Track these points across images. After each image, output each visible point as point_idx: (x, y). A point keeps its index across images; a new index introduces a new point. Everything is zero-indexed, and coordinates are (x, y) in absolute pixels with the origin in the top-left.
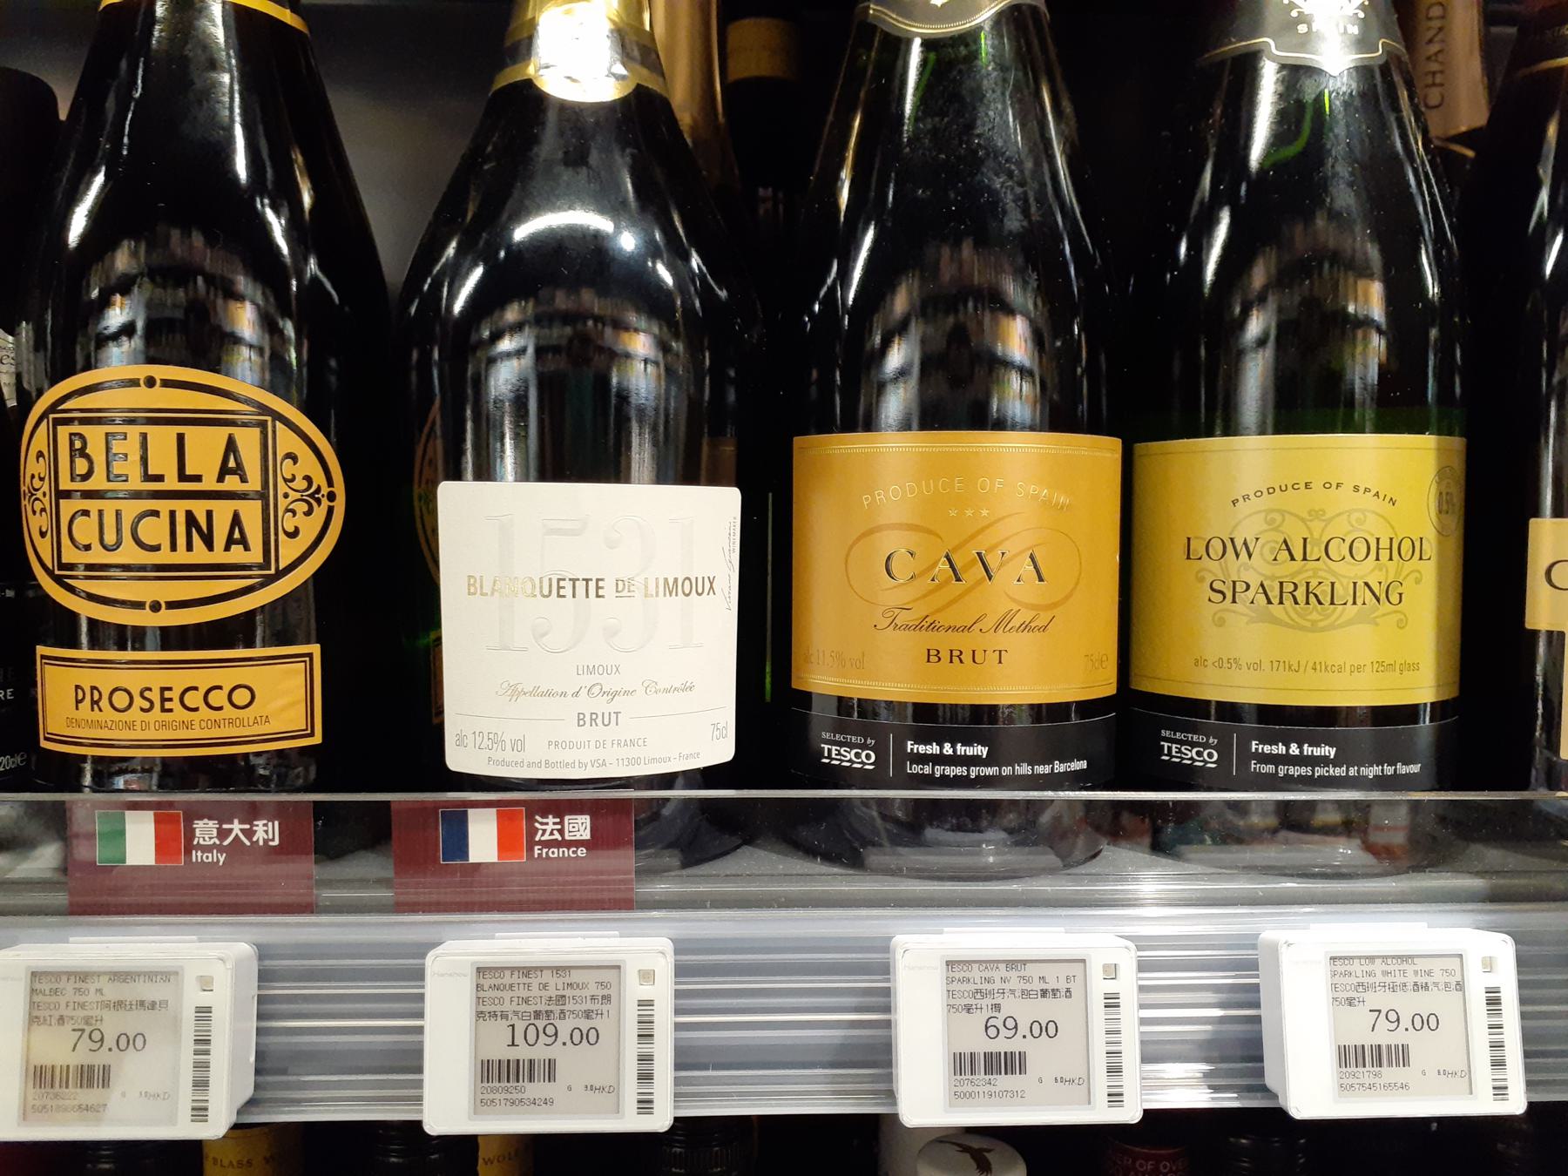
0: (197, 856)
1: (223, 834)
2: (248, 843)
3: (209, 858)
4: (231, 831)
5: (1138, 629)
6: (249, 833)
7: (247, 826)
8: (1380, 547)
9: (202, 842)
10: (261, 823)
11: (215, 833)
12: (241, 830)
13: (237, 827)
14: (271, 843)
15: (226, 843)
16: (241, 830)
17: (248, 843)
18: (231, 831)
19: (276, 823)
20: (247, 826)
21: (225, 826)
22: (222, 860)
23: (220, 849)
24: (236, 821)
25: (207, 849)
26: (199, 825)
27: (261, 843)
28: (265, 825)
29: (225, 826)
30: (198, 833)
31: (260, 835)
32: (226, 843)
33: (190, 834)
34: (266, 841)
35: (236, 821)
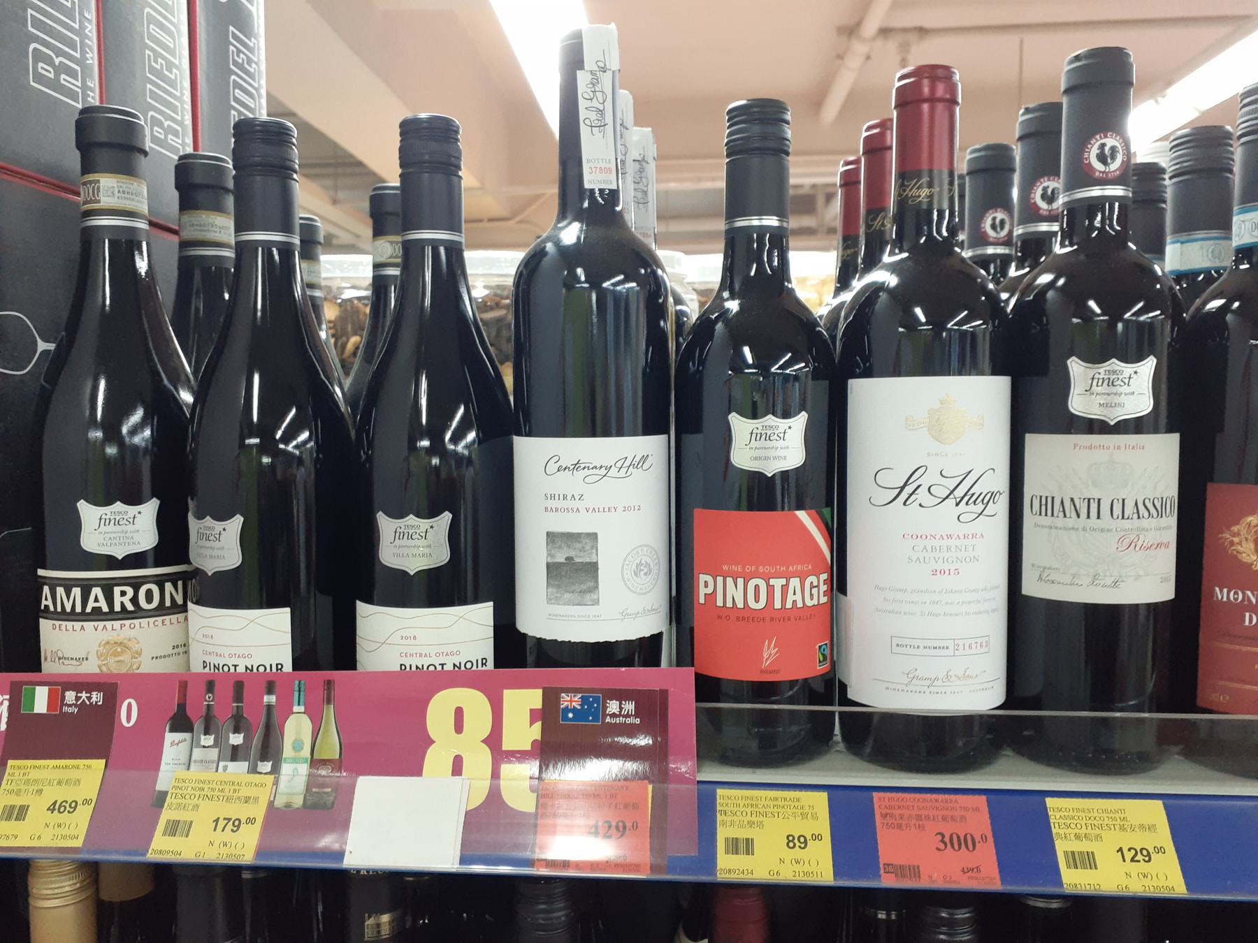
0: (65, 709)
1: (77, 698)
2: (88, 703)
3: (70, 710)
4: (81, 697)
5: (668, 571)
6: (89, 698)
7: (88, 695)
8: (949, 492)
9: (68, 703)
10: (94, 693)
11: (74, 698)
12: (86, 697)
13: (84, 695)
14: (99, 703)
15: (79, 703)
16: (86, 697)
17: (88, 703)
18: (81, 697)
19: (102, 693)
20: (88, 695)
21: (79, 695)
22: (76, 711)
23: (76, 705)
24: (84, 692)
25: (70, 706)
26: (67, 694)
27: (94, 703)
28: (97, 694)
29: (79, 695)
30: (66, 698)
31: (94, 699)
32: (79, 703)
33: (63, 697)
34: (96, 702)
35: (84, 692)
